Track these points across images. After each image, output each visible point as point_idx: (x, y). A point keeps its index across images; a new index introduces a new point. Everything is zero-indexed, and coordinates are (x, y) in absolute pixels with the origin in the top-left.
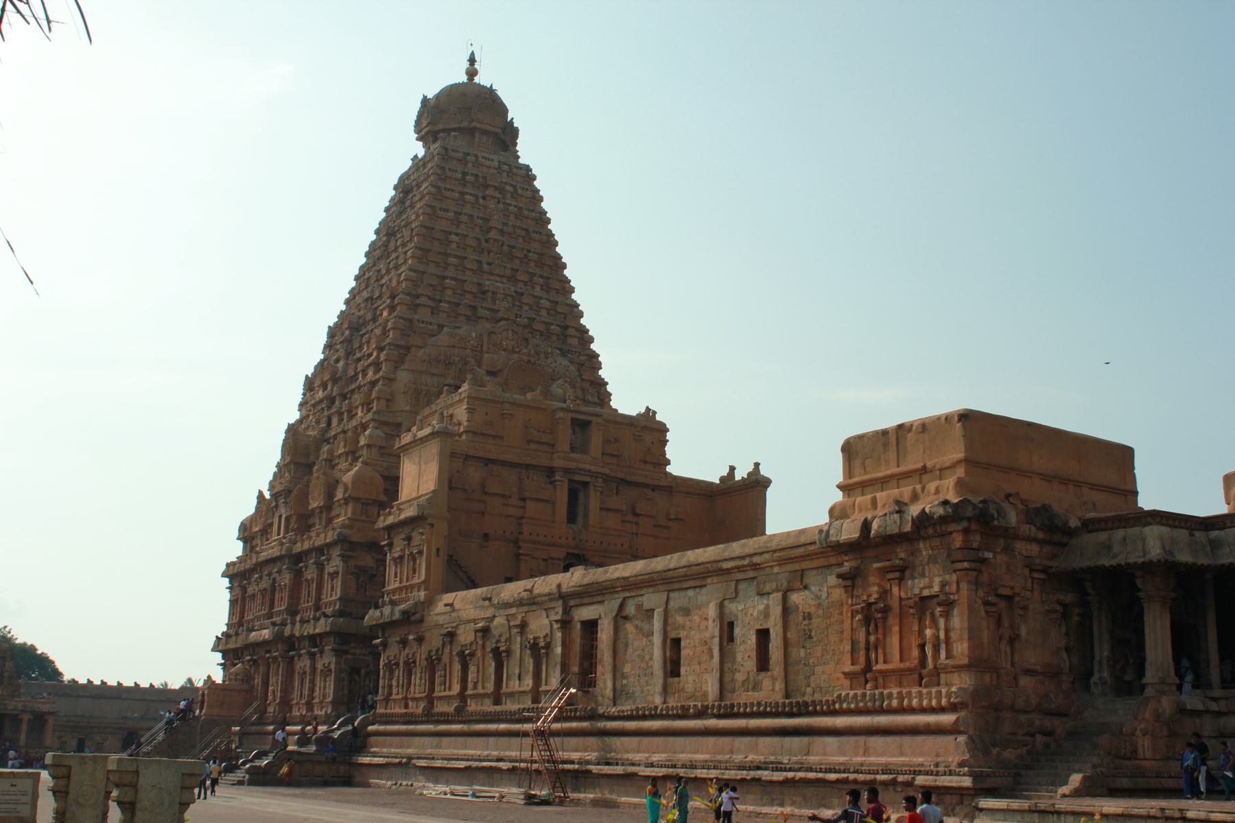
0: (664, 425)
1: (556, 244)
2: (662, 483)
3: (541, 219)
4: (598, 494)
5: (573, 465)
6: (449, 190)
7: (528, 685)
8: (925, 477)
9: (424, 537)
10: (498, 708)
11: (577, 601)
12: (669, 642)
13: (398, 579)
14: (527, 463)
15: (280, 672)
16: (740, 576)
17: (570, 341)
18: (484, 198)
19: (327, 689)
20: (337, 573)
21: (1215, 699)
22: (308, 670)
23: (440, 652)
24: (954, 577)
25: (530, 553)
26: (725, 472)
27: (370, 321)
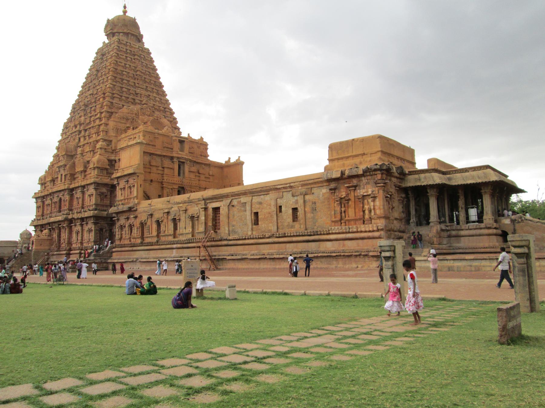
1: (160, 78)
2: (207, 163)
4: (188, 166)
5: (180, 156)
6: (121, 55)
8: (364, 157)
9: (135, 180)
11: (211, 201)
12: (253, 213)
13: (123, 196)
15: (67, 232)
16: (284, 190)
17: (167, 113)
18: (134, 59)
19: (92, 236)
20: (92, 195)
21: (447, 226)
22: (80, 231)
23: (146, 221)
24: (377, 189)
26: (227, 159)
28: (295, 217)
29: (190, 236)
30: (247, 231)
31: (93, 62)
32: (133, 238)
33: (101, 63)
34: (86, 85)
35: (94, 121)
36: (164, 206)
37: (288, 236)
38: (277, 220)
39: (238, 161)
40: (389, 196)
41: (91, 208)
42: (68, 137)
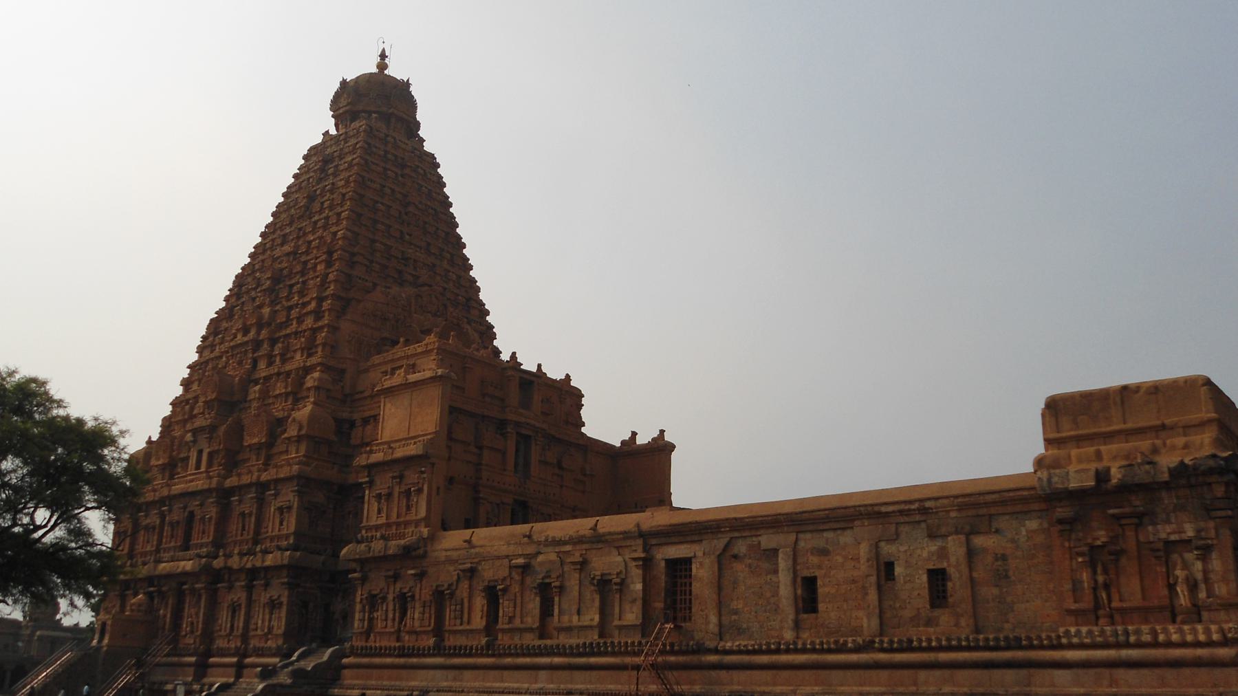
5: (523, 420)
7: (592, 620)
9: (425, 475)
10: (549, 642)
12: (799, 580)
13: (384, 515)
15: (203, 605)
18: (402, 176)
20: (289, 508)
23: (454, 587)
24: (1211, 524)
26: (627, 436)
27: (297, 273)
29: (594, 637)
30: (782, 628)
31: (296, 176)
32: (410, 633)
33: (321, 179)
34: (274, 233)
35: (298, 318)
36: (512, 547)
37: (921, 649)
38: (880, 601)
42: (221, 357)
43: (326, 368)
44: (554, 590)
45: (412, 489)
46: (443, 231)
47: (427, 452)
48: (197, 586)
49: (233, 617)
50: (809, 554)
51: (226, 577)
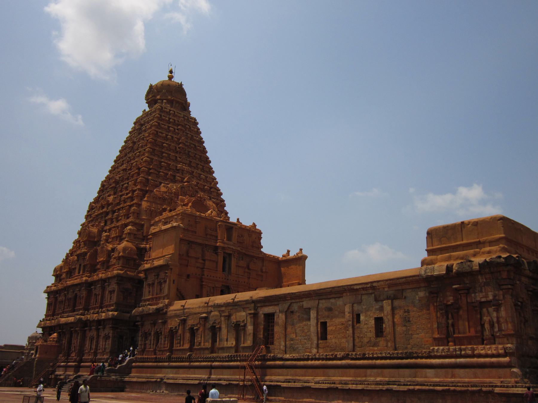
0: (260, 231)
2: (260, 256)
3: (200, 141)
4: (235, 259)
5: (226, 246)
6: (163, 124)
7: (232, 344)
12: (319, 323)
14: (207, 244)
15: (79, 338)
16: (364, 292)
18: (178, 129)
23: (177, 328)
24: (501, 292)
25: (207, 284)
26: (285, 252)
28: (379, 330)
30: (311, 348)
31: (130, 133)
32: (159, 351)
33: (139, 134)
35: (124, 200)
38: (353, 333)
39: (300, 255)
40: (519, 303)
41: (112, 308)
43: (134, 224)
44: (217, 330)
45: (162, 281)
46: (198, 155)
47: (168, 263)
48: (77, 329)
49: (91, 343)
50: (324, 311)
51: (89, 324)
